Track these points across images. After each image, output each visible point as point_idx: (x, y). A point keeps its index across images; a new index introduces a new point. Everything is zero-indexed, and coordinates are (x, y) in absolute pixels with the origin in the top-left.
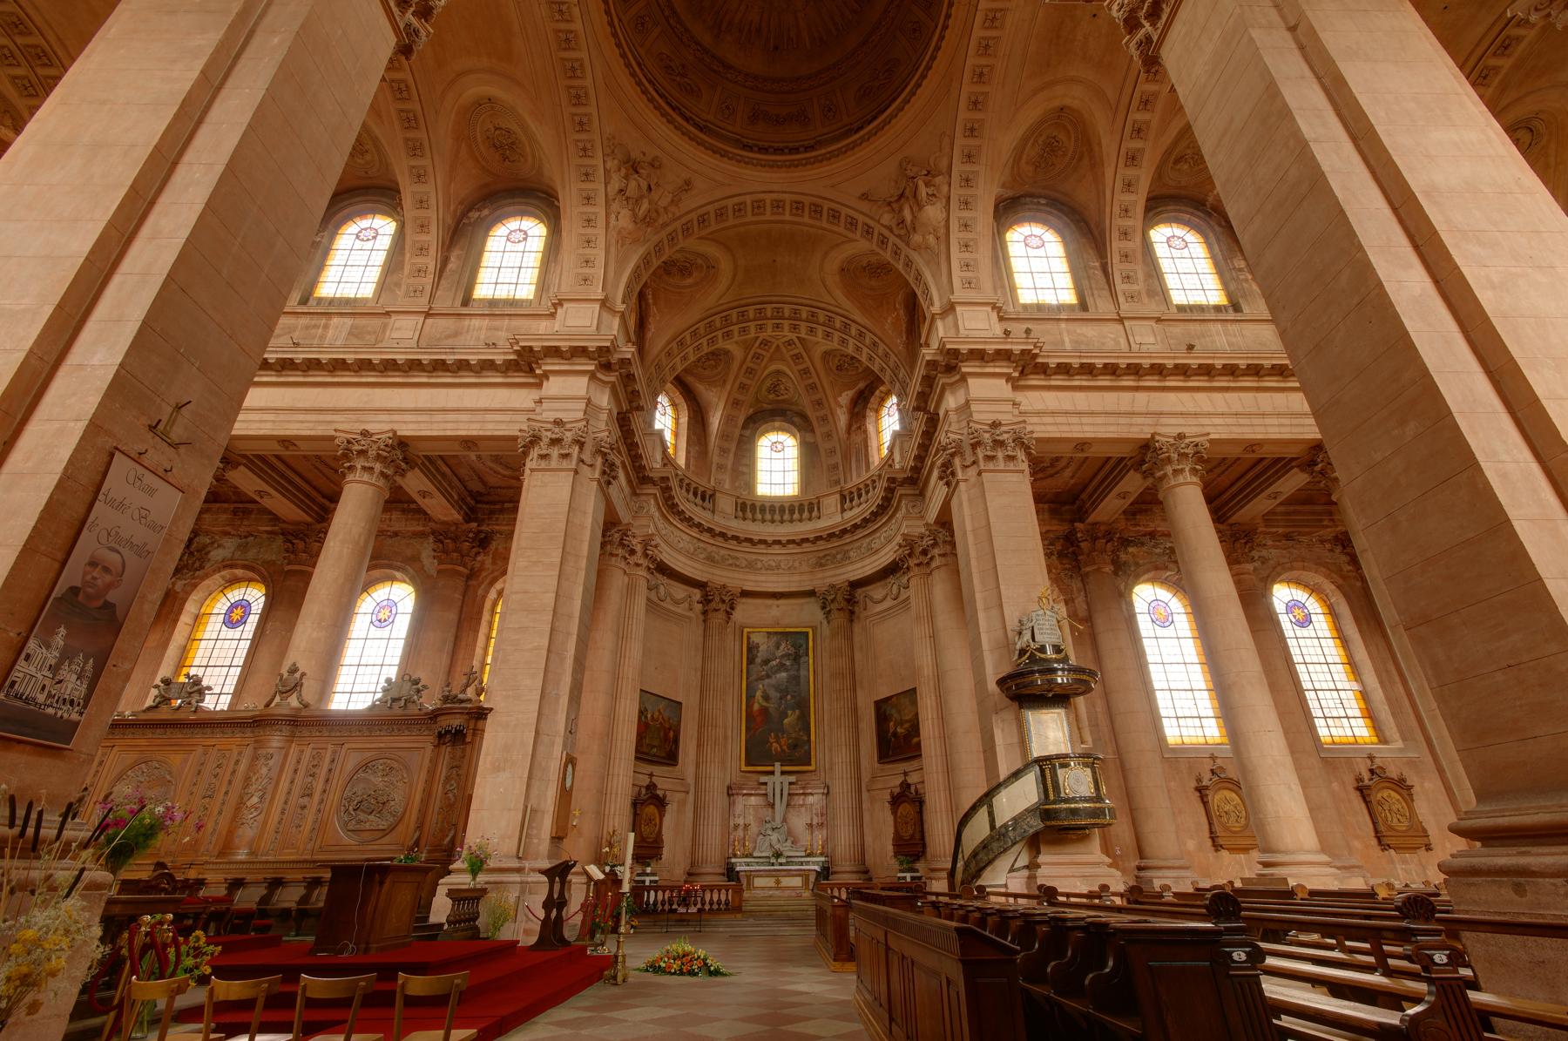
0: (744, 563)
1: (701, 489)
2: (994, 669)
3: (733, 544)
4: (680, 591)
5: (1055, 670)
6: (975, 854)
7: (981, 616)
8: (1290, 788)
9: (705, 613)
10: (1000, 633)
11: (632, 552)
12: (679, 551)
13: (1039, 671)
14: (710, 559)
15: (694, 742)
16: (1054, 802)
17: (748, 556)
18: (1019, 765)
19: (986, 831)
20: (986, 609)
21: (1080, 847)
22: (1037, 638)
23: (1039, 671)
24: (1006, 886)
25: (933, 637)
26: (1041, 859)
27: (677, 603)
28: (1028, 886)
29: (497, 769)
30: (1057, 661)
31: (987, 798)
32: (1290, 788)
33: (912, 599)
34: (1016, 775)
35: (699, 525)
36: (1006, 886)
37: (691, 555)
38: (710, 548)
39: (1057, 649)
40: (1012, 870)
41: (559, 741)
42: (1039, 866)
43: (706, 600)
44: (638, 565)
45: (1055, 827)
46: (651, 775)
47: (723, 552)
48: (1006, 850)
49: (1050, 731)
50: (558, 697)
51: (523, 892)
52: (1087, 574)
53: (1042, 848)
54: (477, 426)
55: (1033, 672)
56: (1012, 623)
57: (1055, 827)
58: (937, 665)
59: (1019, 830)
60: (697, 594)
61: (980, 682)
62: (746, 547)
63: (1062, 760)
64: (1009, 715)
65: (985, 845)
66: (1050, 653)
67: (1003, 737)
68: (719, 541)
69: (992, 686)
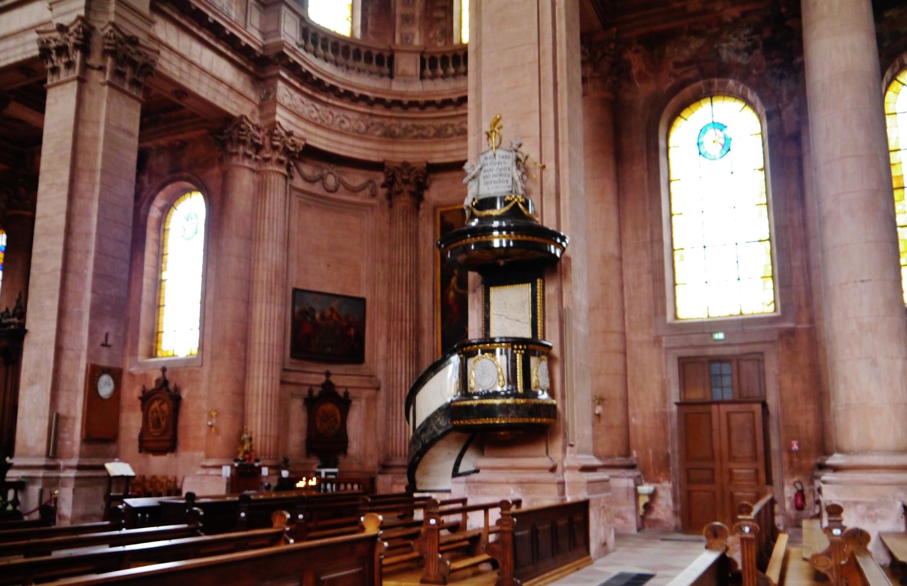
0: (432, 131)
1: (375, 53)
3: (414, 113)
4: (356, 178)
8: (874, 363)
9: (389, 197)
11: (258, 148)
12: (342, 133)
14: (390, 136)
15: (383, 339)
17: (437, 123)
27: (354, 191)
29: (32, 383)
32: (874, 363)
35: (363, 98)
37: (358, 135)
38: (387, 122)
41: (84, 355)
43: (388, 184)
44: (267, 160)
46: (328, 374)
47: (404, 123)
50: (80, 315)
51: (44, 486)
54: (20, 50)
60: (381, 178)
62: (430, 113)
68: (397, 112)
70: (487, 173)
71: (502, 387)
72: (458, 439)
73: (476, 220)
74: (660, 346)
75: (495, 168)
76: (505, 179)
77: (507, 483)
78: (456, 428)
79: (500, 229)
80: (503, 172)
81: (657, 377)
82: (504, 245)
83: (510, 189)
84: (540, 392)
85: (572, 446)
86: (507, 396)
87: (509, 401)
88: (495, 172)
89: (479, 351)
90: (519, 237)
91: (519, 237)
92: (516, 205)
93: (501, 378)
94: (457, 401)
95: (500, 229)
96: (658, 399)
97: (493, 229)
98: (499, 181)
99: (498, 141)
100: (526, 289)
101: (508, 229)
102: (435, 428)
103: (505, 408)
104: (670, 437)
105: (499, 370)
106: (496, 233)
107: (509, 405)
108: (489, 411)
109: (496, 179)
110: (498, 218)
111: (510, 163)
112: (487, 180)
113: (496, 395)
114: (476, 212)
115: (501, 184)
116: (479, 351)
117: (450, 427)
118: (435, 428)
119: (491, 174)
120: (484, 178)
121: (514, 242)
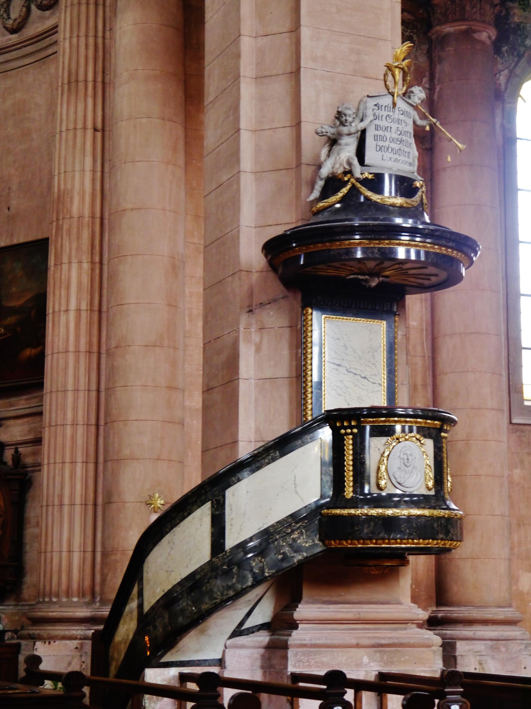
2: (259, 214)
5: (396, 231)
6: (169, 599)
7: (247, 91)
10: (284, 136)
13: (364, 230)
16: (354, 503)
18: (281, 427)
19: (202, 554)
20: (260, 78)
21: (378, 592)
22: (370, 156)
23: (364, 230)
24: (221, 662)
25: (103, 130)
26: (303, 611)
28: (267, 665)
30: (403, 212)
31: (212, 490)
33: (64, 35)
34: (283, 445)
36: (221, 662)
39: (405, 186)
40: (238, 632)
42: (294, 625)
45: (346, 547)
48: (239, 594)
49: (348, 358)
52: (444, 39)
53: (306, 593)
55: (352, 230)
56: (317, 116)
57: (346, 547)
58: (103, 193)
59: (273, 556)
61: (219, 246)
63: (378, 420)
64: (275, 319)
65: (194, 583)
66: (389, 195)
67: (258, 362)
69: (250, 253)
75: (394, 126)
77: (358, 646)
79: (413, 231)
82: (413, 257)
88: (395, 136)
94: (327, 506)
95: (413, 231)
97: (399, 230)
98: (397, 152)
102: (287, 549)
106: (405, 238)
109: (396, 146)
112: (381, 143)
115: (402, 158)
118: (287, 549)
119: (388, 135)
120: (376, 138)
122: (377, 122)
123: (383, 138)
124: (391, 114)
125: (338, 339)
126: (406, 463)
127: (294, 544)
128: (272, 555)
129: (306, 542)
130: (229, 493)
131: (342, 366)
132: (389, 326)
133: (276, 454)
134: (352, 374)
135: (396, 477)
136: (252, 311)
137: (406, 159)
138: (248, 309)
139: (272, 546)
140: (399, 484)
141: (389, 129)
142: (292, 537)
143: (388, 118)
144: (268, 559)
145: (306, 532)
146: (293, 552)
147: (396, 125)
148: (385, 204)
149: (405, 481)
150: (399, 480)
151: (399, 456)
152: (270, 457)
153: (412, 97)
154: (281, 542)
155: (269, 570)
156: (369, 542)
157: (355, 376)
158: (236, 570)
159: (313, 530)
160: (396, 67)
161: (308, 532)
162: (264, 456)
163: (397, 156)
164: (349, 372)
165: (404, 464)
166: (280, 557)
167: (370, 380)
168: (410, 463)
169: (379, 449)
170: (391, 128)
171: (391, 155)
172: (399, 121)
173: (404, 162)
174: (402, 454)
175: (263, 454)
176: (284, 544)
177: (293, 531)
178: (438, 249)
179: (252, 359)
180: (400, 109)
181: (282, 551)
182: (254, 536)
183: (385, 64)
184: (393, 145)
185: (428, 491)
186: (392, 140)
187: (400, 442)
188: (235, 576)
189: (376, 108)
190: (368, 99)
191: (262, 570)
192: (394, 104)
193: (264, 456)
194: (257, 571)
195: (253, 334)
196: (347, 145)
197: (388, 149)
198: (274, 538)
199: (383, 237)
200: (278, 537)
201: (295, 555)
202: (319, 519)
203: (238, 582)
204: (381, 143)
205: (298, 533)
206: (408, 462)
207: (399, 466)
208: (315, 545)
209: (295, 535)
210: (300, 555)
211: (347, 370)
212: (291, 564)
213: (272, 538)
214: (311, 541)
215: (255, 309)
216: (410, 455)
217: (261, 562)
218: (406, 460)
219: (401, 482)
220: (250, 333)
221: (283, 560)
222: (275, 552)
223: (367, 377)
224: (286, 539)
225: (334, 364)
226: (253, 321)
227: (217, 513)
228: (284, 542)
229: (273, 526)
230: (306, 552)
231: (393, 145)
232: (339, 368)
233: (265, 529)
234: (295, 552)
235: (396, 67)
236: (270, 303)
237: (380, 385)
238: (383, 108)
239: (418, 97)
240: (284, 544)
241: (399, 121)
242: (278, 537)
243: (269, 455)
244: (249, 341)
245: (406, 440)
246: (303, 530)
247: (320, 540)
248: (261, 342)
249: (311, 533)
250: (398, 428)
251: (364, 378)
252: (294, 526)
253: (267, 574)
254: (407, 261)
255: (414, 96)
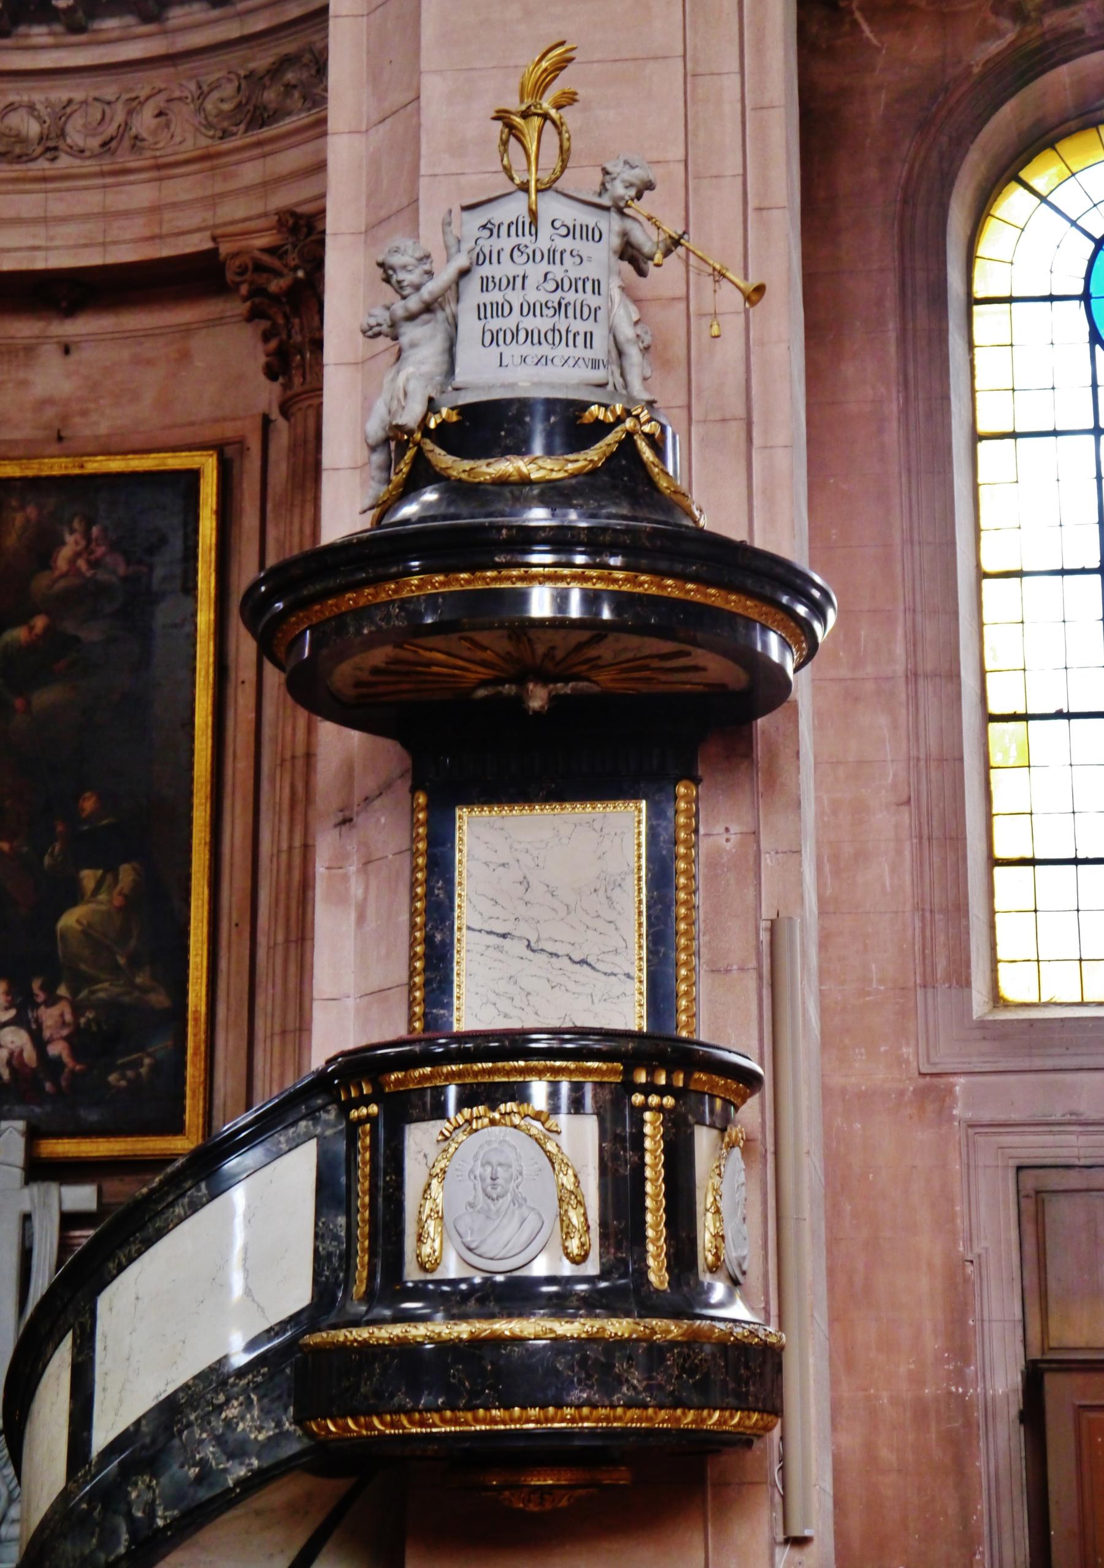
70: (495, 296)
71: (579, 1260)
72: (294, 1511)
73: (430, 496)
74: (943, 1115)
75: (535, 271)
76: (579, 326)
78: (323, 1458)
80: (570, 297)
81: (928, 1245)
82: (575, 611)
83: (599, 375)
84: (719, 1291)
85: (800, 1542)
86: (597, 1302)
87: (618, 1327)
88: (533, 296)
89: (452, 1092)
90: (646, 585)
91: (646, 585)
92: (628, 443)
93: (575, 1217)
95: (561, 540)
96: (932, 1343)
99: (550, 158)
100: (626, 823)
101: (596, 542)
102: (210, 1450)
103: (598, 1362)
104: (982, 1506)
105: (568, 1182)
107: (620, 1343)
108: (484, 1371)
109: (542, 324)
110: (553, 493)
111: (599, 259)
112: (495, 324)
113: (515, 1294)
114: (442, 459)
115: (562, 351)
116: (452, 1092)
117: (292, 1448)
119: (515, 297)
120: (482, 311)
121: (620, 601)
122: (486, 270)
123: (498, 310)
124: (527, 240)
125: (503, 865)
126: (489, 1189)
127: (230, 1437)
128: (175, 1467)
129: (260, 1429)
130: (103, 1301)
131: (513, 937)
132: (656, 813)
133: (199, 1190)
134: (544, 957)
135: (461, 1231)
136: (351, 820)
137: (580, 351)
138: (340, 816)
139: (176, 1442)
140: (470, 1249)
141: (519, 281)
142: (223, 1416)
143: (516, 253)
144: (164, 1480)
145: (259, 1400)
146: (224, 1458)
147: (544, 267)
148: (480, 483)
149: (483, 1241)
150: (468, 1239)
151: (472, 1171)
152: (186, 1200)
153: (608, 186)
154: (197, 1431)
155: (165, 1509)
156: (436, 1417)
157: (554, 959)
158: (100, 1513)
159: (277, 1393)
160: (525, 115)
161: (266, 1401)
162: (170, 1198)
163: (545, 349)
164: (533, 951)
165: (484, 1190)
166: (194, 1471)
167: (598, 966)
168: (499, 1189)
169: (425, 1156)
170: (524, 277)
171: (527, 349)
172: (552, 256)
173: (571, 362)
174: (479, 1162)
175: (167, 1194)
176: (204, 1436)
177: (228, 1401)
178: (626, 580)
179: (349, 946)
180: (557, 224)
181: (198, 1457)
182: (144, 1416)
183: (494, 115)
184: (530, 323)
185: (574, 1266)
186: (531, 309)
187: (476, 1130)
188: (97, 1530)
189: (487, 233)
190: (466, 215)
191: (150, 1511)
192: (533, 214)
193: (170, 1198)
194: (140, 1514)
195: (353, 880)
196: (413, 345)
197: (515, 336)
198: (184, 1421)
199: (394, 570)
200: (192, 1417)
201: (229, 1465)
202: (300, 1366)
203: (101, 1545)
204: (495, 324)
205: (241, 1404)
206: (494, 1186)
207: (471, 1199)
208: (281, 1435)
209: (231, 1412)
210: (242, 1464)
211: (529, 946)
212: (218, 1490)
213: (180, 1421)
214: (273, 1425)
215: (358, 814)
216: (500, 1164)
217: (149, 1487)
218: (489, 1181)
219: (473, 1246)
220: (345, 878)
221: (199, 1480)
222: (182, 1459)
223: (589, 960)
224: (209, 1423)
225: (490, 933)
226: (352, 846)
227: (80, 1359)
228: (203, 1431)
229: (185, 1387)
230: (259, 1458)
231: (530, 323)
232: (507, 943)
233: (168, 1397)
234: (231, 1456)
235: (525, 115)
236: (381, 794)
237: (628, 976)
238: (504, 229)
239: (623, 181)
240: (204, 1436)
241: (552, 256)
242: (192, 1417)
243: (183, 1195)
244: (340, 899)
245: (493, 1122)
246: (254, 1397)
247: (298, 1421)
248: (365, 899)
249: (273, 1401)
250: (539, 1090)
251: (583, 962)
252: (234, 1385)
253: (160, 1522)
254: (559, 624)
255: (614, 179)
